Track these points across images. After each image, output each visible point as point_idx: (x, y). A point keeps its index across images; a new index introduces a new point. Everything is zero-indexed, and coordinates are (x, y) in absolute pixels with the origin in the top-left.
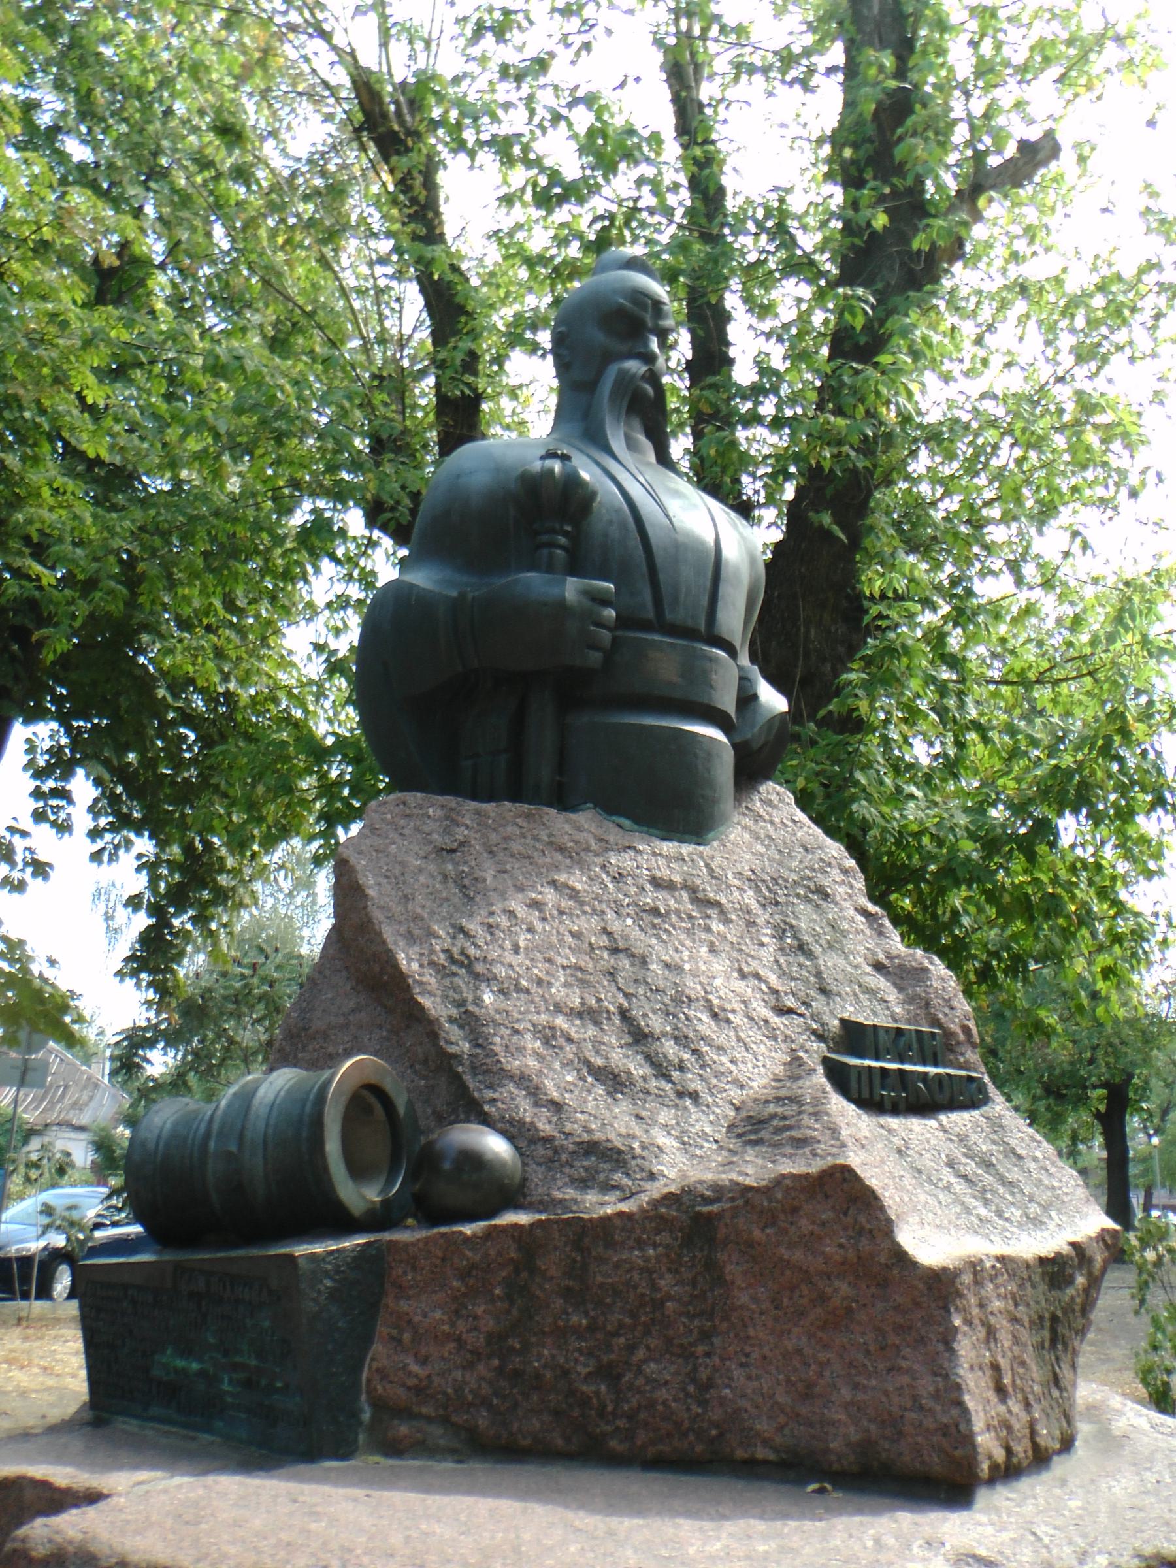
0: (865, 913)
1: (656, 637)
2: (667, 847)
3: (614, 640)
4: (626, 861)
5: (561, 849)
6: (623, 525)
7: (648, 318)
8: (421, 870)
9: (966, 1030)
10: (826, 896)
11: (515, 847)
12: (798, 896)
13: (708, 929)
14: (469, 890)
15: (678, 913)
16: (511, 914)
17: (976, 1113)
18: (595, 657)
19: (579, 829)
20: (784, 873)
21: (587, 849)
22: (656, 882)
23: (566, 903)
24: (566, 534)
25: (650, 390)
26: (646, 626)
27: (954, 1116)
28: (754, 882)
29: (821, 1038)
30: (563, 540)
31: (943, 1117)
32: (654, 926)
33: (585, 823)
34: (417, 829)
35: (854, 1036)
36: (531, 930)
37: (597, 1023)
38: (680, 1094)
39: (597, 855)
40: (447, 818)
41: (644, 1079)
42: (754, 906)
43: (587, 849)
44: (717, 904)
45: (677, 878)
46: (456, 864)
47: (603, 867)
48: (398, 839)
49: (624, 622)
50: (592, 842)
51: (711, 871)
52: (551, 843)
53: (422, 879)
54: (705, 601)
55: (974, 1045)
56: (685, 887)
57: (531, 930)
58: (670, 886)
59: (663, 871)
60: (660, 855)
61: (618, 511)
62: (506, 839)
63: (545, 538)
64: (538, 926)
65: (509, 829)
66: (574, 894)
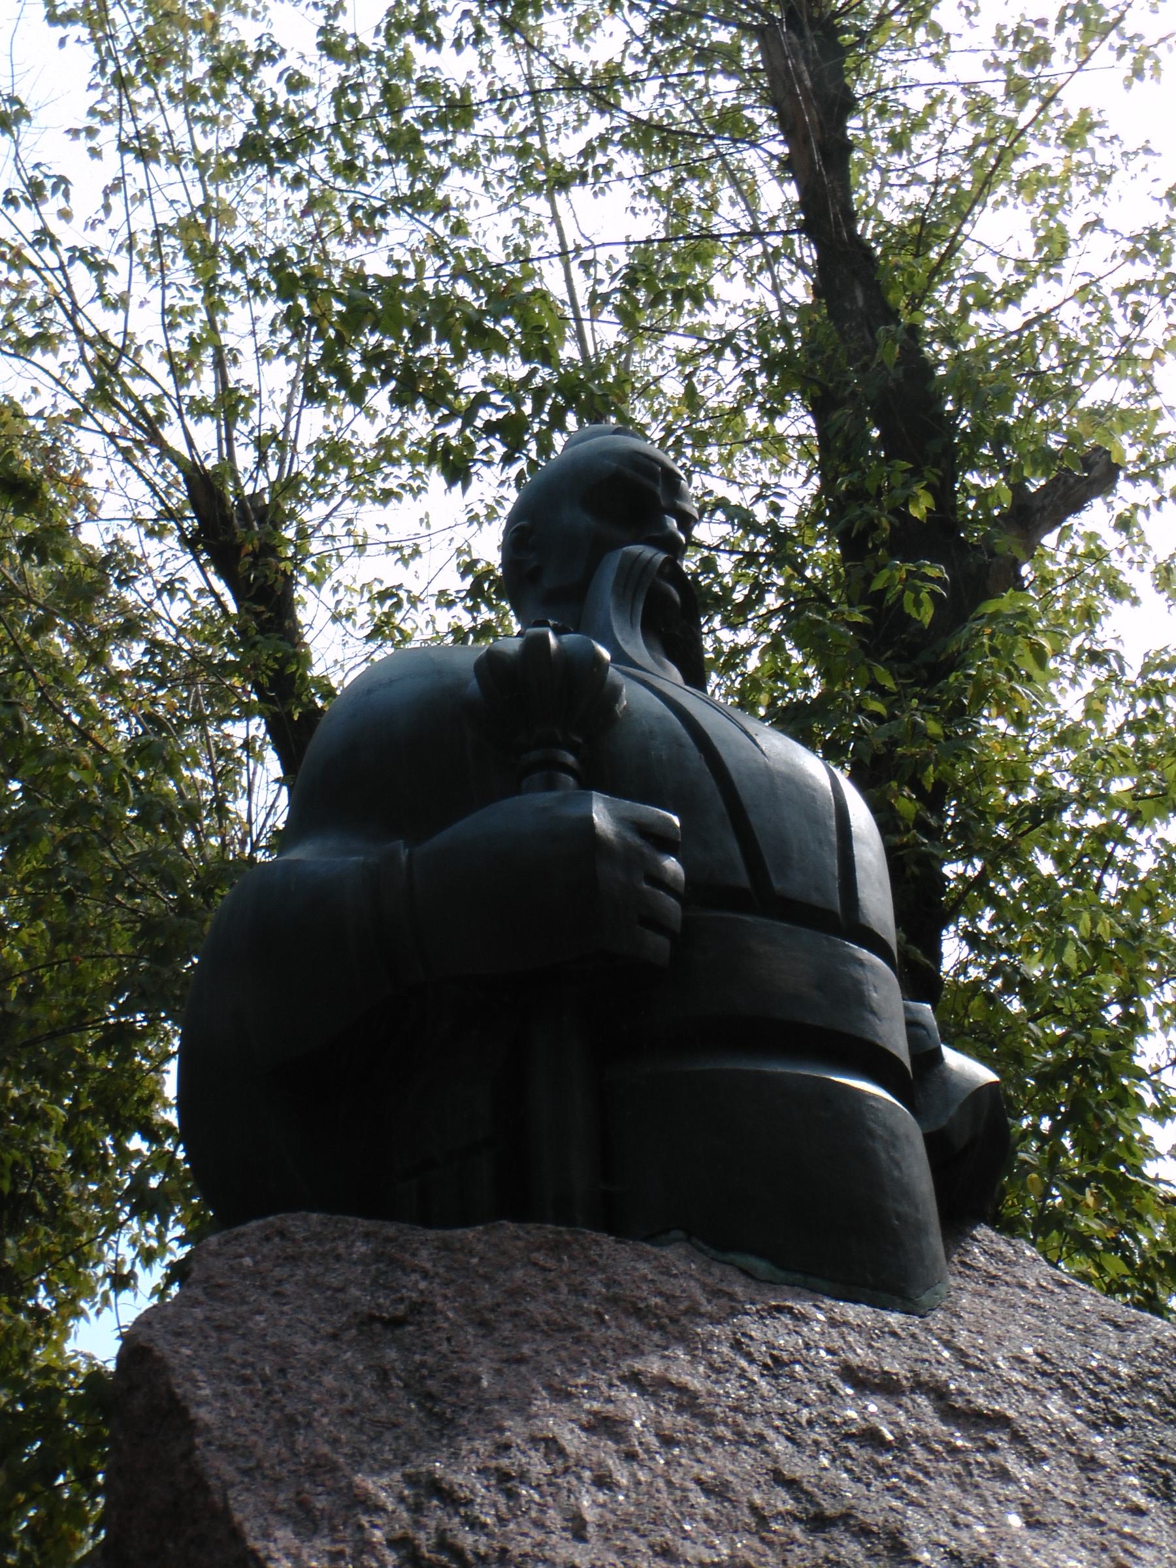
2: (853, 1312)
5: (639, 1313)
13: (1004, 1475)
16: (552, 1447)
18: (658, 945)
21: (694, 1312)
23: (674, 1421)
24: (574, 750)
26: (738, 900)
32: (880, 1470)
33: (669, 1270)
34: (314, 1283)
36: (603, 1482)
40: (378, 1257)
43: (694, 1312)
44: (1000, 1421)
46: (406, 1350)
47: (737, 1346)
48: (272, 1306)
49: (700, 890)
51: (961, 1355)
52: (614, 1300)
53: (329, 1380)
54: (833, 864)
56: (919, 1386)
57: (603, 1482)
61: (661, 719)
62: (514, 1293)
65: (519, 1274)
66: (687, 1401)
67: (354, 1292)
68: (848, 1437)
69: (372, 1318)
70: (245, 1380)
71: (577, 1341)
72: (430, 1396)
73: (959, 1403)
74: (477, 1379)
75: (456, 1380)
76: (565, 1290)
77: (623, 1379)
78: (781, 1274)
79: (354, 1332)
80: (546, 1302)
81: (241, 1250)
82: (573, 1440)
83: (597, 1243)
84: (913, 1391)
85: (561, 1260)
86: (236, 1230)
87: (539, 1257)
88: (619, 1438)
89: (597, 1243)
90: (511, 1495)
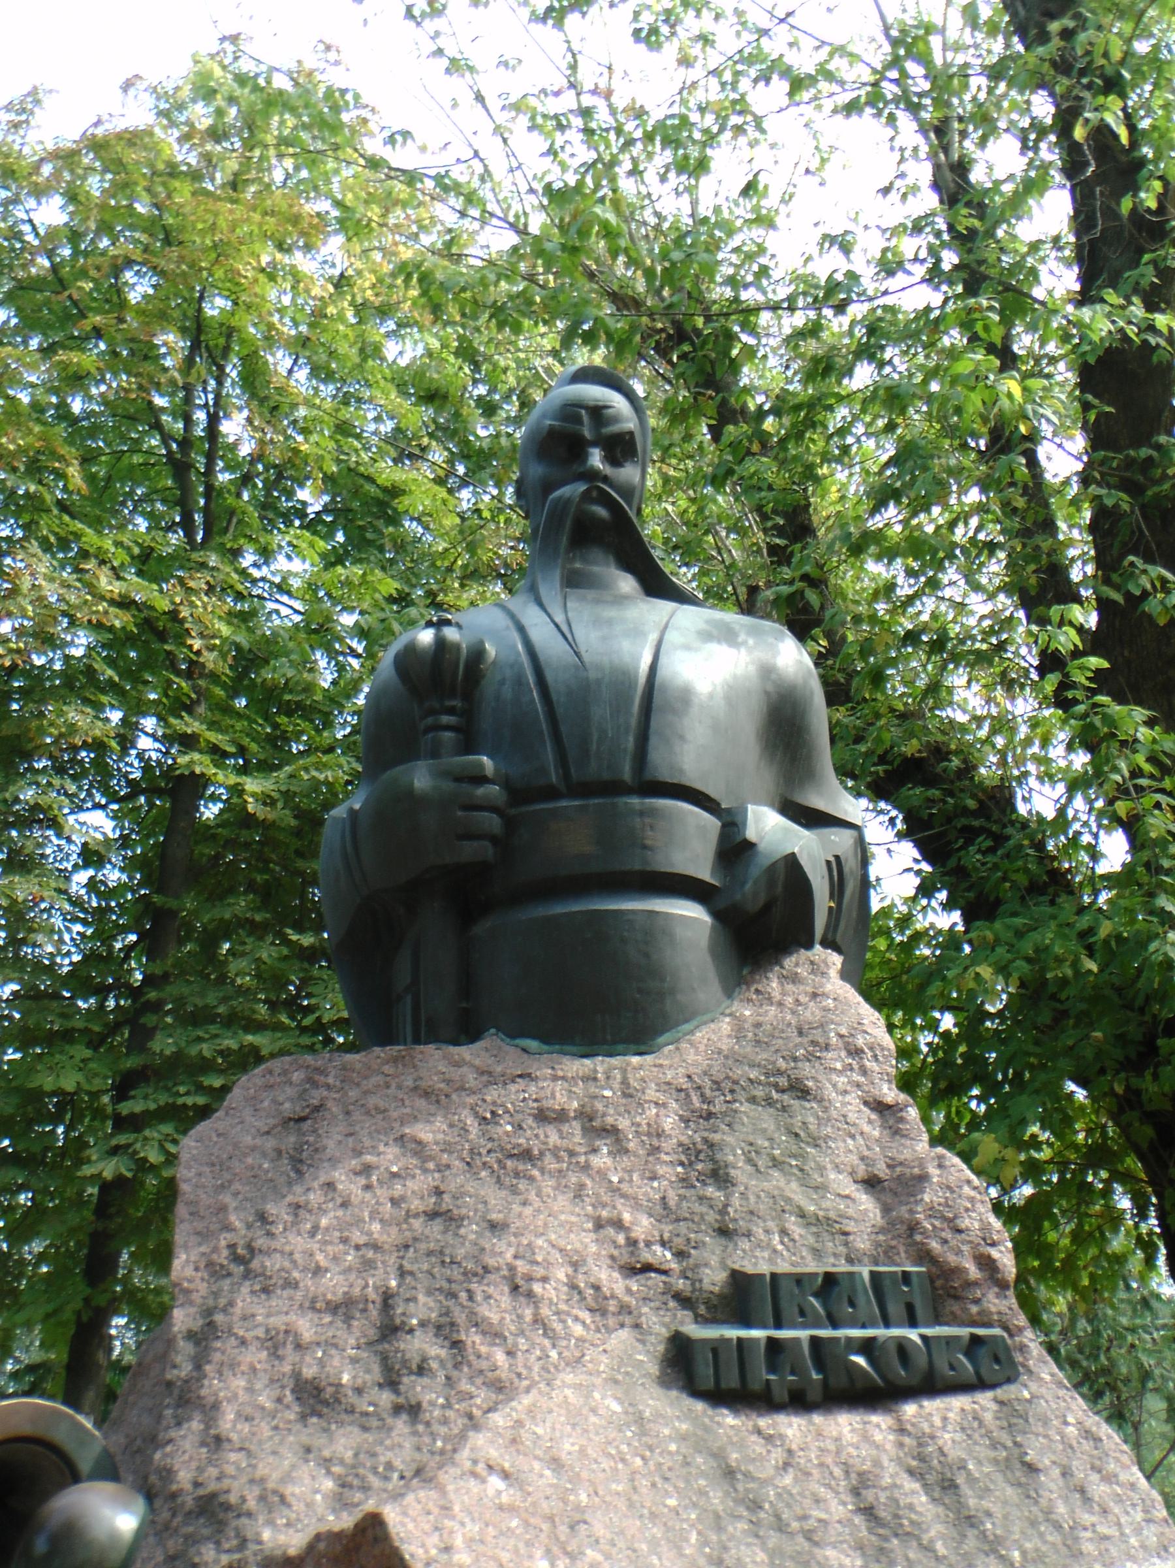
0: (880, 1107)
1: (564, 803)
4: (513, 1095)
5: (426, 1094)
7: (587, 433)
8: (253, 1149)
9: (987, 1264)
10: (802, 1092)
12: (753, 1100)
13: (586, 1167)
14: (300, 1164)
15: (555, 1152)
16: (330, 1186)
17: (985, 1399)
19: (457, 1064)
22: (542, 1116)
24: (451, 711)
25: (602, 512)
26: (551, 793)
27: (933, 1406)
29: (685, 1301)
31: (910, 1409)
35: (742, 1297)
37: (348, 1318)
38: (397, 1409)
41: (359, 1391)
42: (669, 1122)
44: (612, 1132)
53: (249, 1160)
54: (630, 742)
55: (1003, 1285)
59: (560, 1097)
60: (568, 1079)
68: (511, 1156)
78: (545, 1047)
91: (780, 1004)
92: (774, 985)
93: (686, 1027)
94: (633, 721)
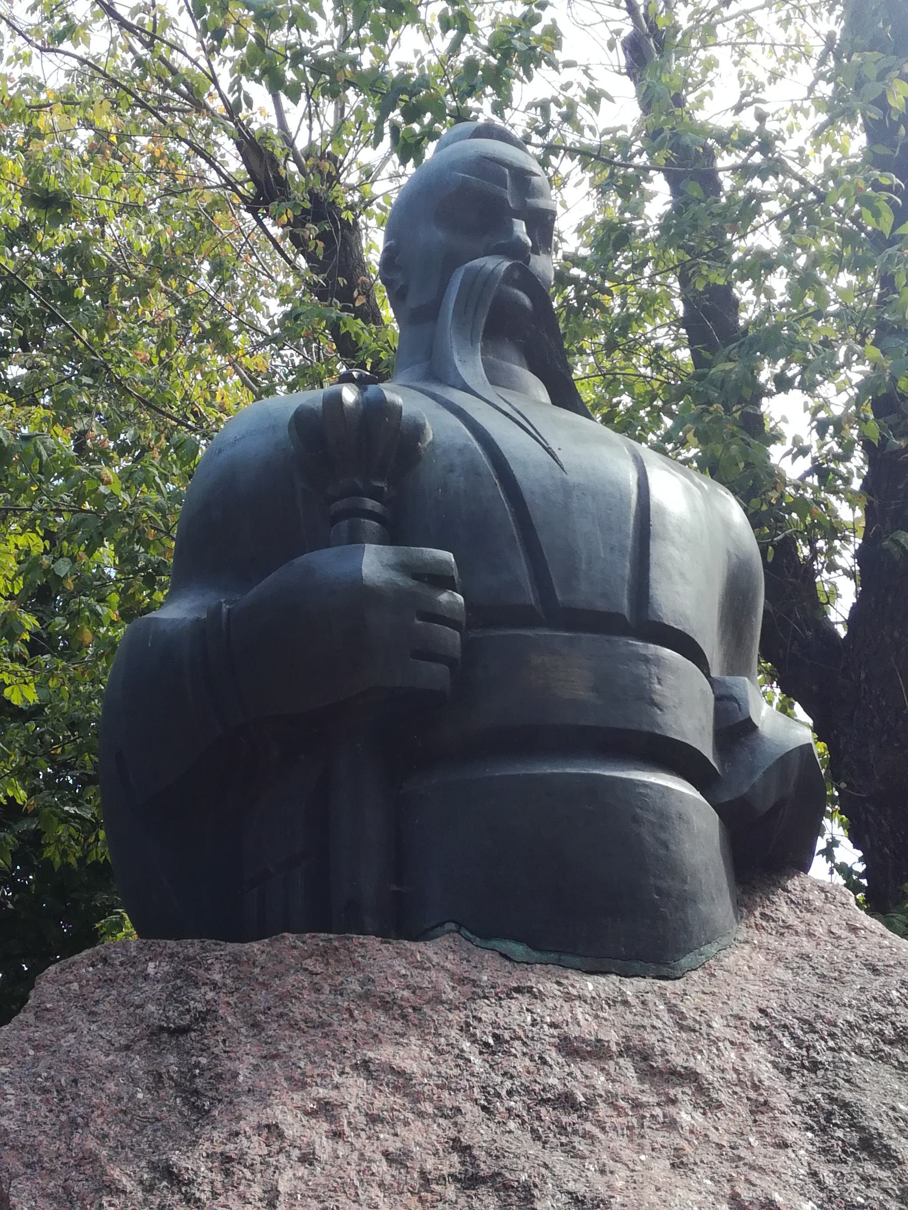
2: (590, 985)
3: (467, 644)
4: (515, 1014)
5: (386, 1005)
6: (473, 470)
8: (112, 1070)
11: (297, 1010)
12: (859, 1050)
13: (672, 1124)
14: (200, 1098)
16: (273, 1130)
18: (435, 674)
20: (831, 1011)
22: (570, 1048)
23: (382, 1102)
24: (376, 494)
26: (524, 617)
28: (767, 1029)
30: (371, 504)
33: (437, 961)
39: (453, 1007)
40: (178, 974)
42: (766, 1072)
44: (691, 1076)
45: (612, 1037)
47: (465, 1028)
49: (480, 614)
50: (446, 985)
52: (366, 996)
53: (111, 1086)
54: (626, 569)
56: (627, 1050)
57: (308, 1159)
58: (597, 1052)
59: (584, 1024)
61: (463, 450)
63: (342, 504)
64: (324, 1147)
65: (291, 979)
66: (402, 1082)
67: (151, 1008)
68: (544, 1102)
69: (161, 1029)
70: (46, 1091)
71: (326, 1036)
72: (196, 1092)
73: (659, 1063)
74: (235, 1075)
75: (219, 1077)
76: (327, 989)
77: (355, 1067)
78: (536, 955)
79: (145, 1042)
80: (309, 1004)
81: (71, 977)
82: (293, 1126)
83: (363, 945)
84: (621, 1055)
85: (328, 964)
86: (70, 960)
87: (309, 963)
88: (332, 1119)
89: (363, 945)
90: (228, 1173)
91: (810, 935)
92: (784, 911)
93: (711, 949)
94: (629, 543)
